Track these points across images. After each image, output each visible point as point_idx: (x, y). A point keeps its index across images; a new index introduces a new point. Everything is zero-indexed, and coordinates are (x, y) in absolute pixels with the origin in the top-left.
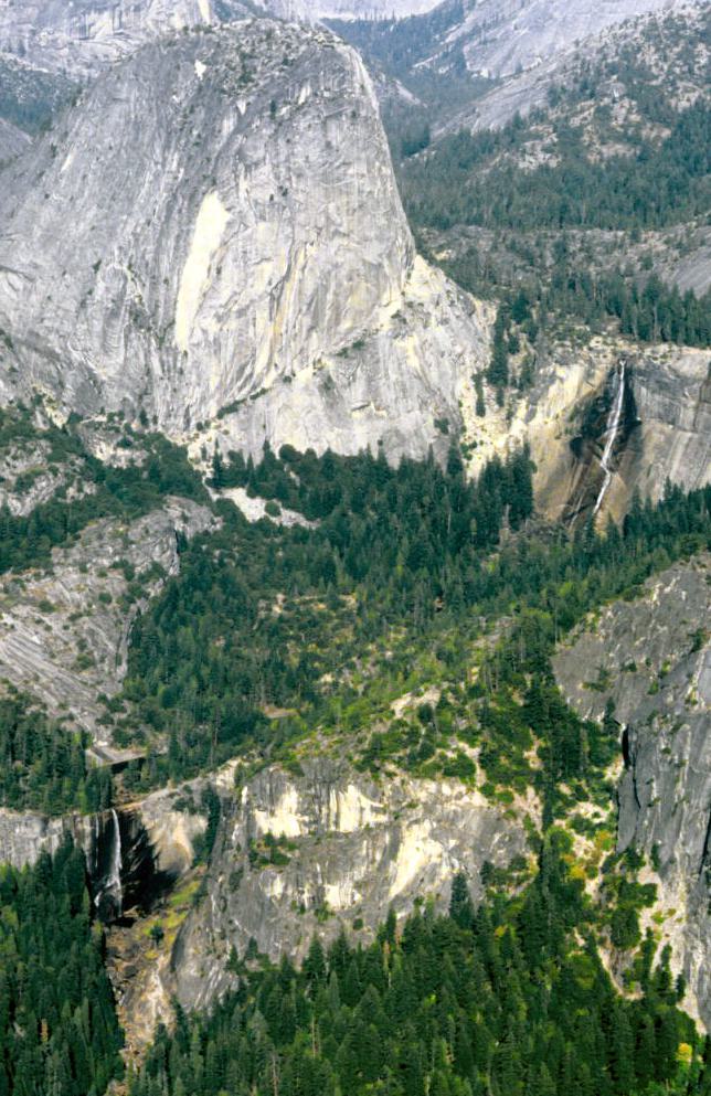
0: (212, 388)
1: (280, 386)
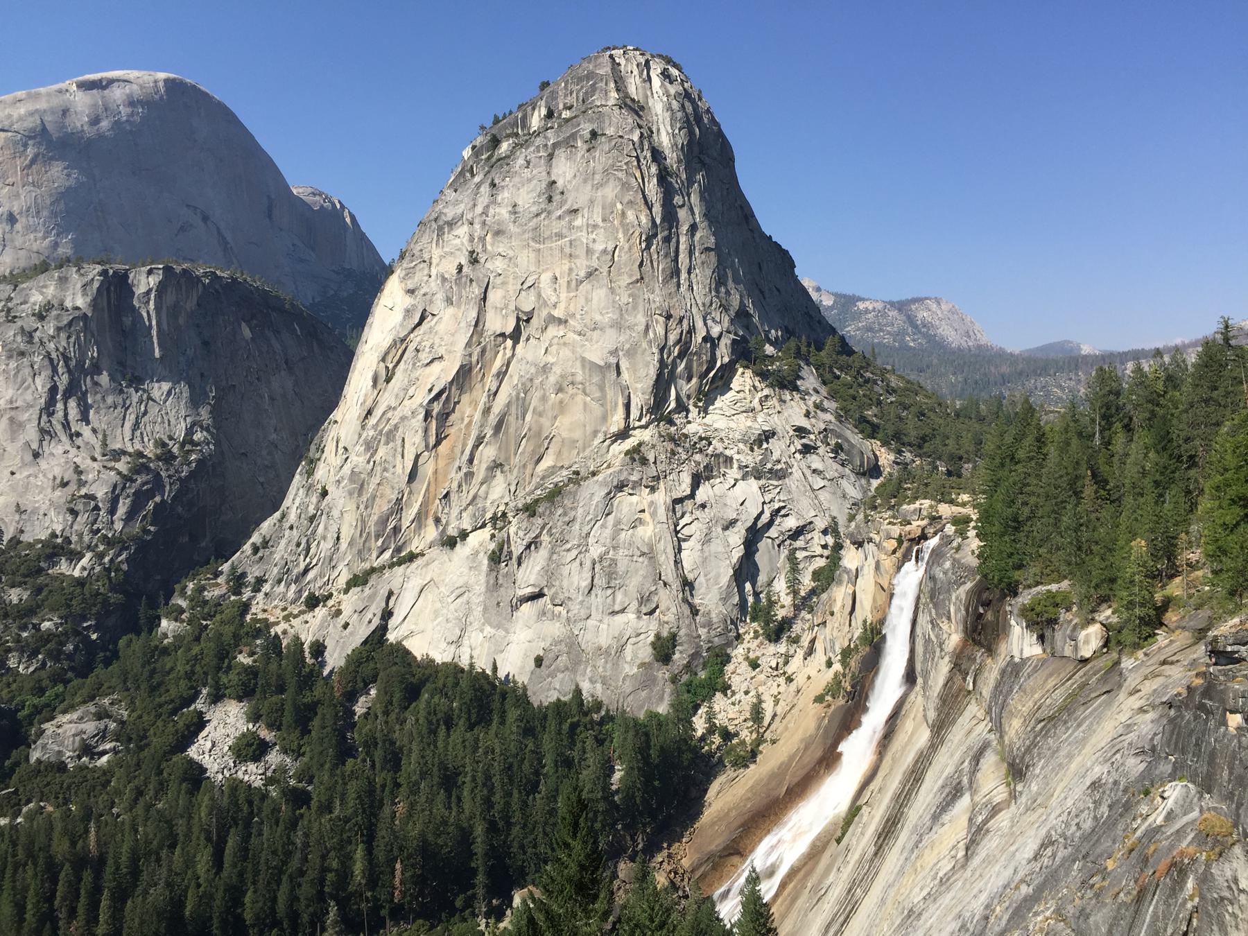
0: (344, 545)
1: (435, 551)
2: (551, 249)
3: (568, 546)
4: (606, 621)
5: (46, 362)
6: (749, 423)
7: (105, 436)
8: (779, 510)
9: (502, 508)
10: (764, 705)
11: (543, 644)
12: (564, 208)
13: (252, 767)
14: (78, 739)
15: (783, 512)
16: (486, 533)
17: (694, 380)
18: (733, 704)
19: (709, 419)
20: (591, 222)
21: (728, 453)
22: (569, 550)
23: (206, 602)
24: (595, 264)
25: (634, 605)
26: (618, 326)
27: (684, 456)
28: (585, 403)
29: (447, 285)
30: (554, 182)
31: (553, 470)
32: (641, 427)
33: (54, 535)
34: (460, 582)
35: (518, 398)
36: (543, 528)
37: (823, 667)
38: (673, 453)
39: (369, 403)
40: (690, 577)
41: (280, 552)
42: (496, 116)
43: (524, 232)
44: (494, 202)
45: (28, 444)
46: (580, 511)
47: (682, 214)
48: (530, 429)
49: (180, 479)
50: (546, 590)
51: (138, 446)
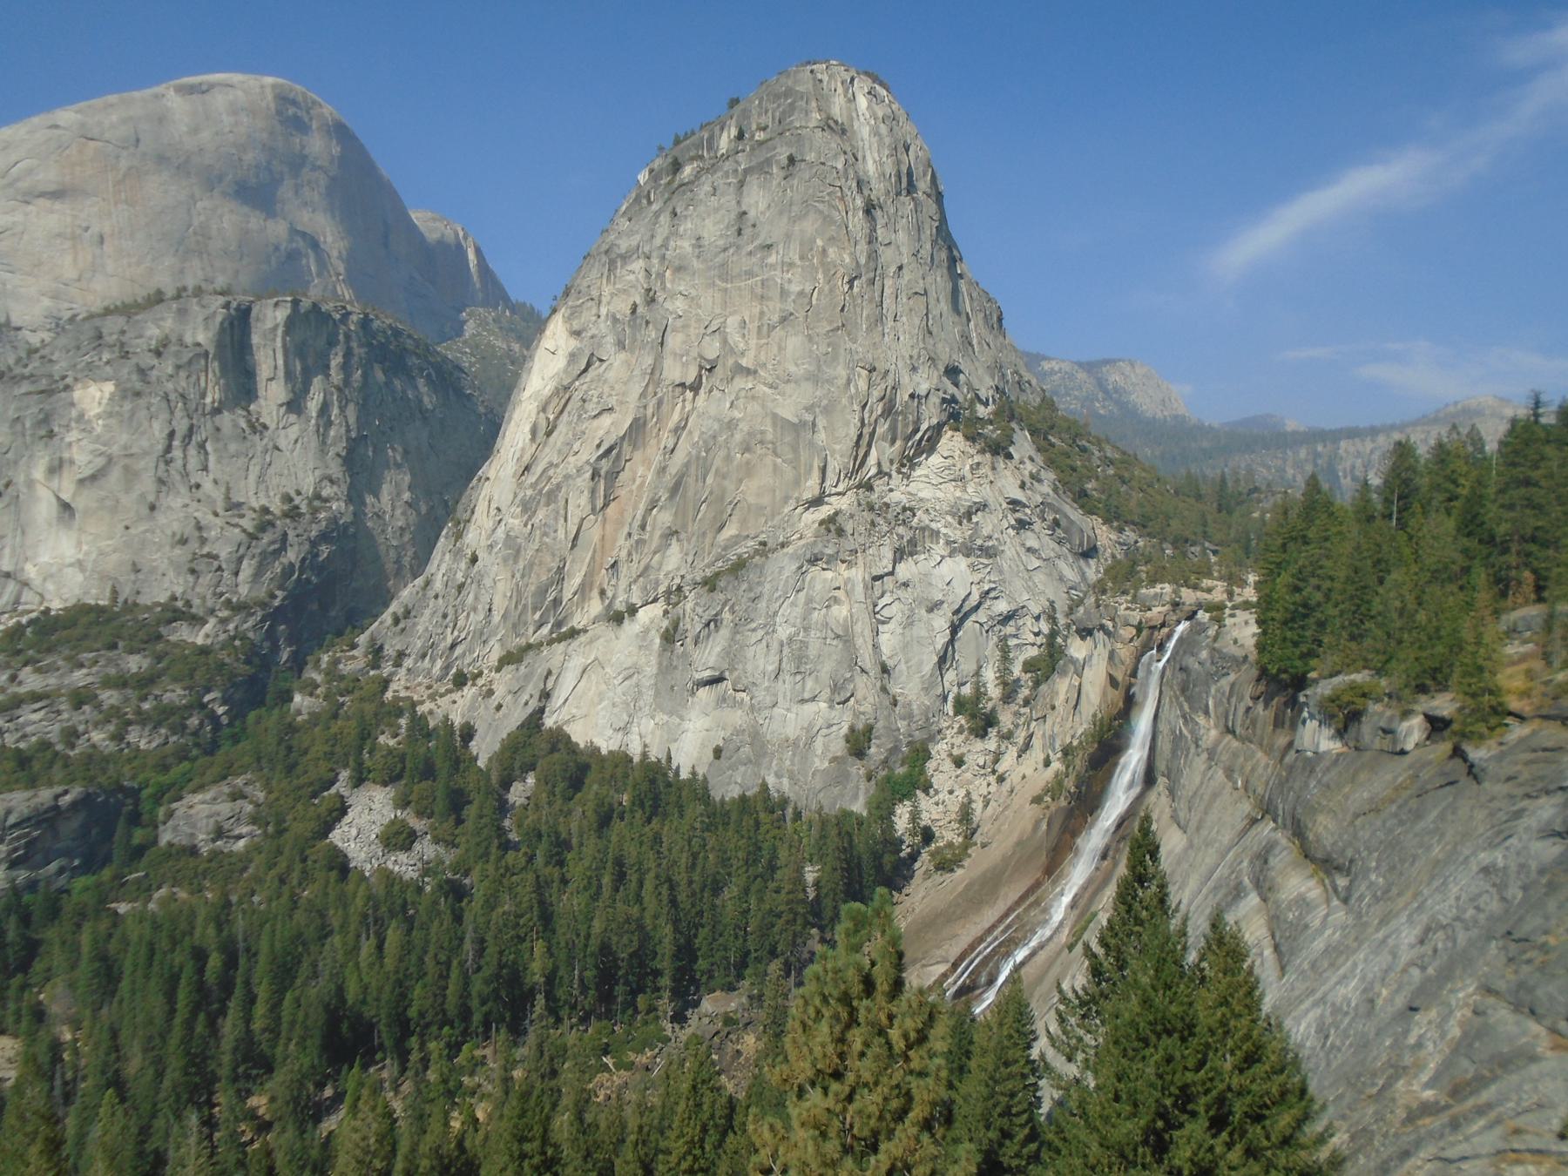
0: (496, 617)
1: (601, 628)
2: (740, 289)
3: (753, 625)
4: (794, 709)
5: (164, 404)
6: (958, 494)
7: (228, 489)
8: (987, 592)
9: (677, 581)
10: (974, 806)
11: (722, 734)
12: (756, 243)
13: (402, 857)
14: (212, 820)
15: (992, 595)
16: (657, 609)
17: (898, 443)
18: (937, 804)
19: (913, 487)
20: (786, 260)
21: (934, 526)
22: (754, 630)
23: (342, 678)
24: (790, 307)
25: (826, 693)
26: (814, 378)
27: (885, 528)
28: (775, 465)
29: (619, 327)
30: (745, 213)
31: (736, 540)
32: (838, 494)
33: (174, 598)
34: (629, 662)
35: (698, 458)
36: (724, 605)
37: (1041, 766)
38: (873, 524)
39: (526, 459)
40: (890, 663)
41: (424, 622)
42: (677, 136)
43: (709, 269)
44: (676, 234)
45: (143, 496)
46: (768, 586)
47: (886, 255)
48: (711, 493)
49: (309, 539)
50: (727, 674)
51: (264, 501)
